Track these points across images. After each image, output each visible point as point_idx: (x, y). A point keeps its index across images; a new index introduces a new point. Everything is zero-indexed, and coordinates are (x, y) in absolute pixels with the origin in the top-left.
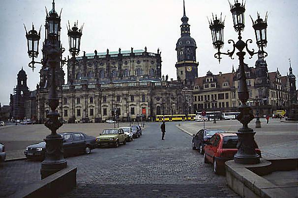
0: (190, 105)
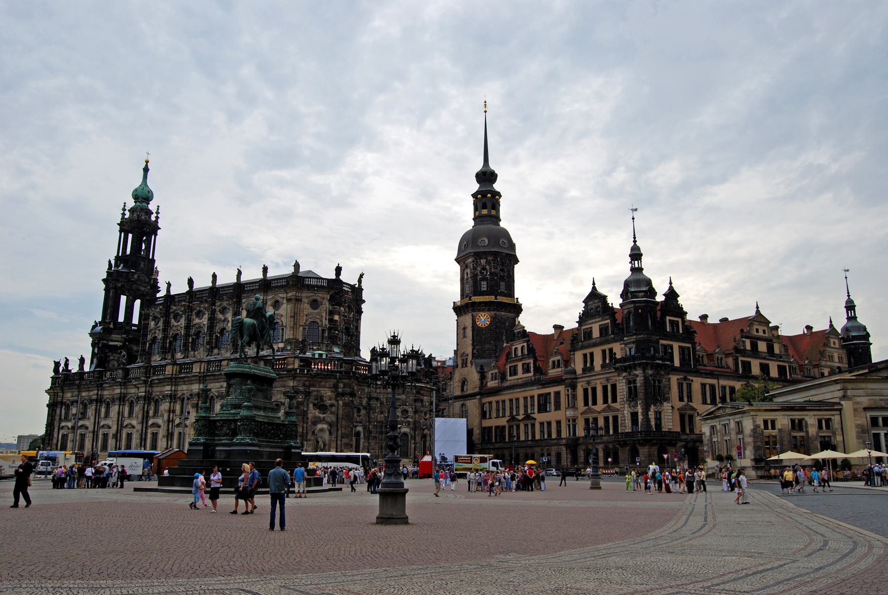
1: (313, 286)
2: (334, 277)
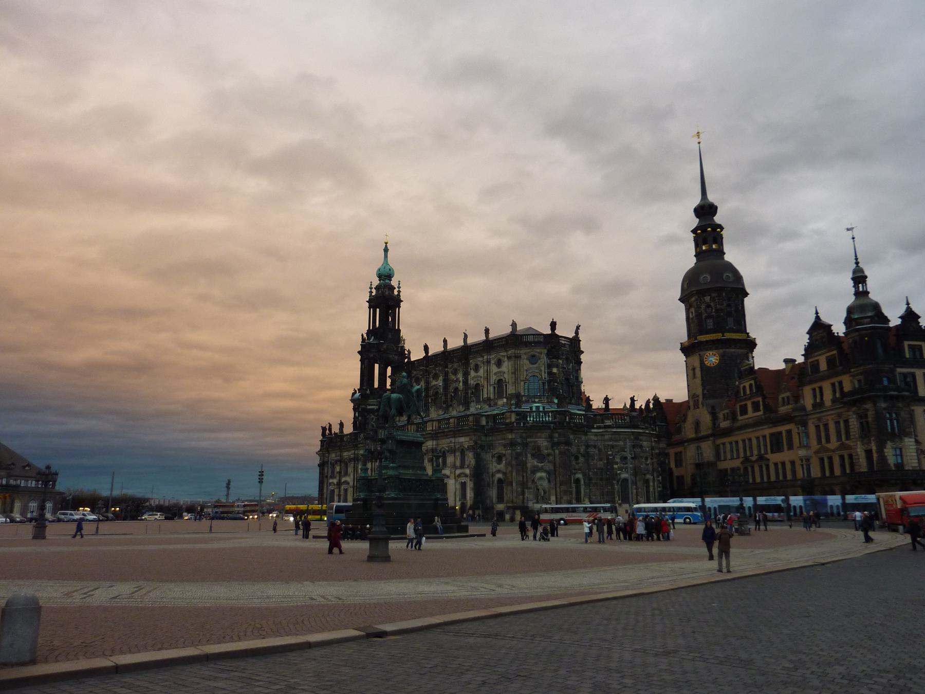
0: (624, 476)
1: (530, 343)
2: (549, 332)
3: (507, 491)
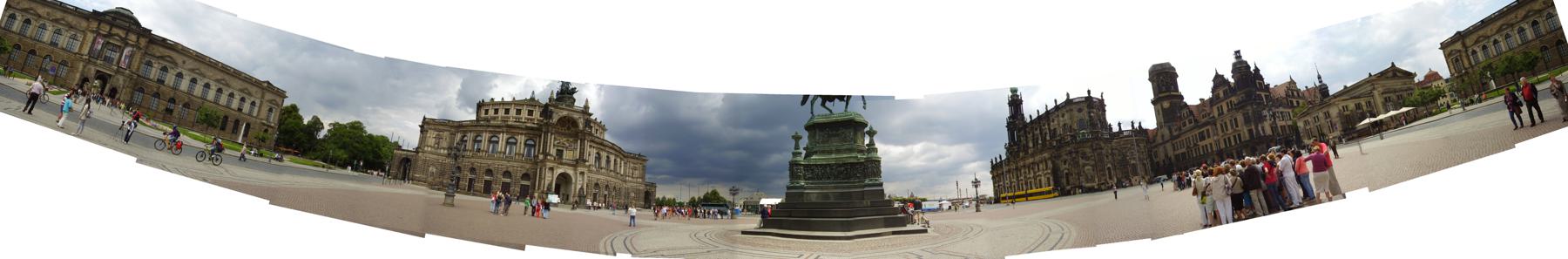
0: (1133, 162)
3: (1070, 178)
